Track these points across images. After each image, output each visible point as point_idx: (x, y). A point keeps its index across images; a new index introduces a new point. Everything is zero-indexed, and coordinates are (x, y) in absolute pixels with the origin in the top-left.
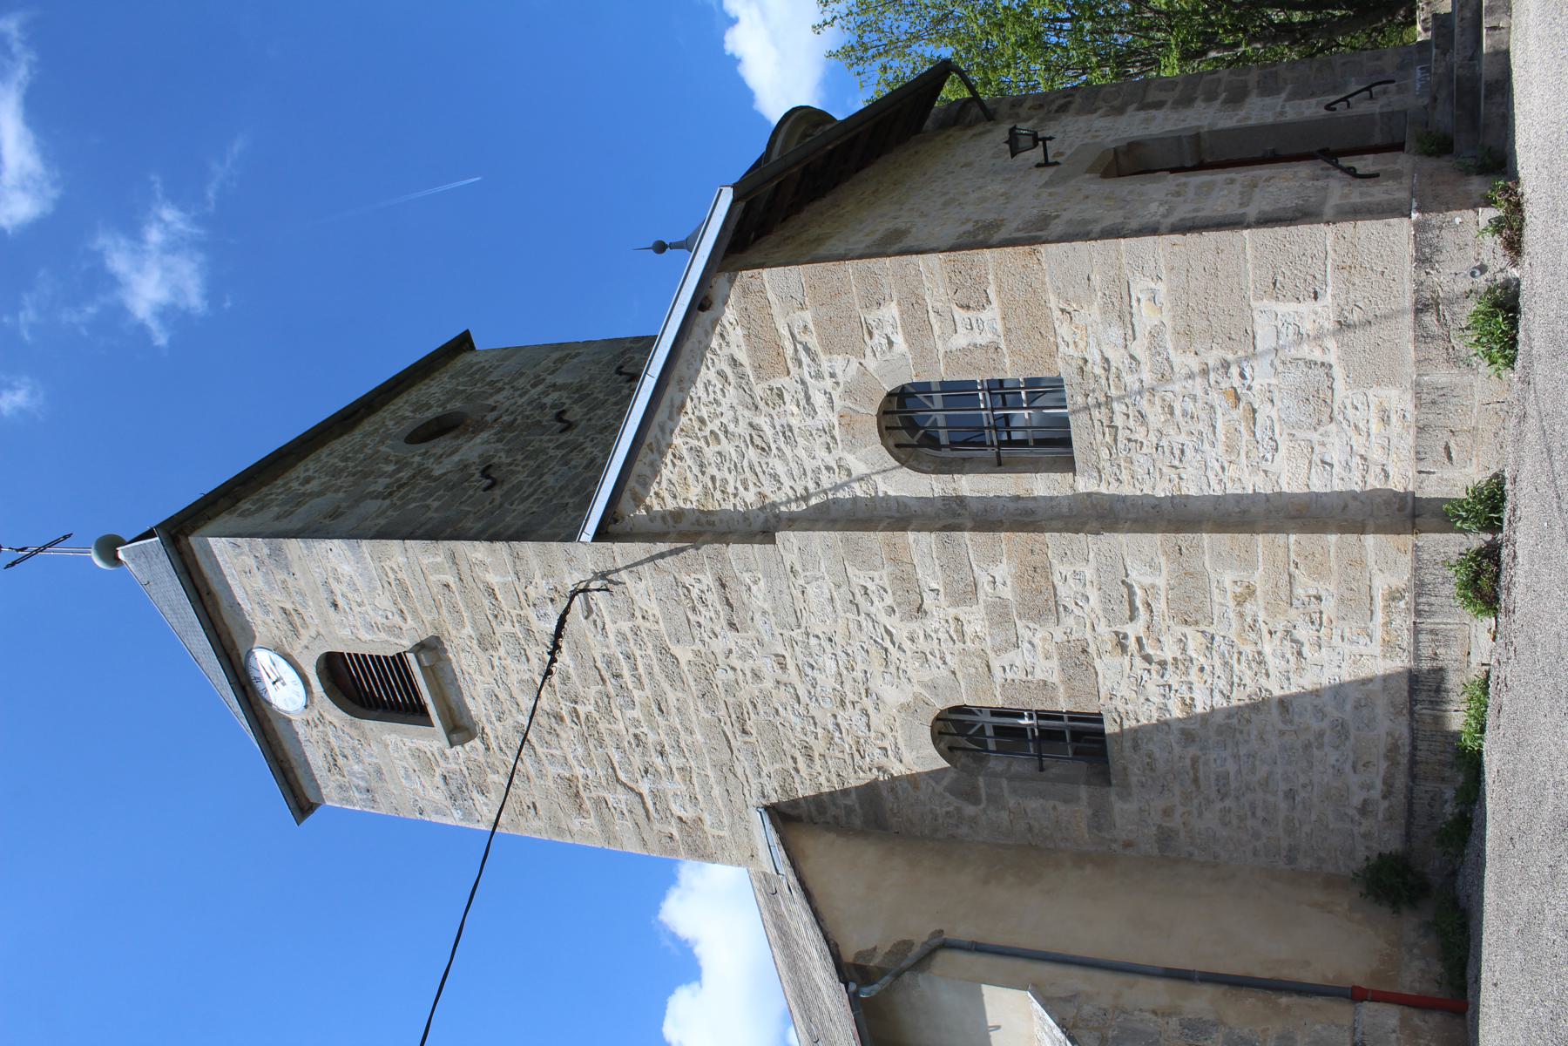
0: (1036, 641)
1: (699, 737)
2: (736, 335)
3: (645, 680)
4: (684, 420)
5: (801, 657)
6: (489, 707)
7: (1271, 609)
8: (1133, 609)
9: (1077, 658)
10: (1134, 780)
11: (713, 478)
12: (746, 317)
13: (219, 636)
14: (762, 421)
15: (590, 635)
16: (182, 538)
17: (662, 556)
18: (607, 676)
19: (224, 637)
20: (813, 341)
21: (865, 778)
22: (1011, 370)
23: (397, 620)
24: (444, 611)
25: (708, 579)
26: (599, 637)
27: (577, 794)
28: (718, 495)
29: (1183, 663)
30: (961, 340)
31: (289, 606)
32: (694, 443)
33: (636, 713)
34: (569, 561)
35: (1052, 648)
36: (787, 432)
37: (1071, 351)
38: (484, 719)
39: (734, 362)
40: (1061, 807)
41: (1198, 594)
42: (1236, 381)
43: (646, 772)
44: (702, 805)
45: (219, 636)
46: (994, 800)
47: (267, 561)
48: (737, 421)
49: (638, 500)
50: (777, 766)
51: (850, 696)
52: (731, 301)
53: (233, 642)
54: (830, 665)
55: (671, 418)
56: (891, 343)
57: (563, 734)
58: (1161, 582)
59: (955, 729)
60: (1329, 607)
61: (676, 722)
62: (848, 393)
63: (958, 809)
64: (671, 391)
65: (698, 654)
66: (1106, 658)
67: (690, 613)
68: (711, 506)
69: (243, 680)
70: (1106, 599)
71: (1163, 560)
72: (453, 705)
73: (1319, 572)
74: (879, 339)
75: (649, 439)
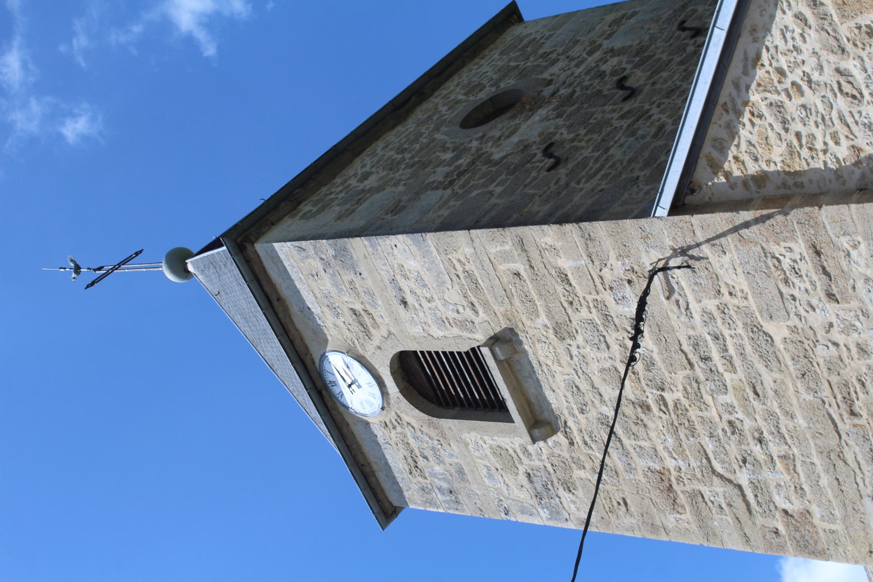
1: (801, 421)
3: (737, 362)
4: (760, 73)
6: (571, 399)
11: (798, 135)
13: (292, 342)
14: (851, 65)
15: (673, 317)
16: (248, 245)
17: (746, 225)
18: (694, 359)
19: (297, 342)
23: (469, 313)
24: (517, 302)
25: (800, 247)
26: (683, 318)
27: (670, 488)
28: (805, 153)
31: (358, 307)
32: (773, 97)
33: (729, 398)
34: (645, 238)
38: (566, 412)
43: (744, 461)
44: (809, 495)
45: (292, 342)
47: (333, 262)
48: (821, 68)
49: (716, 167)
53: (306, 347)
55: (745, 73)
57: (650, 424)
65: (794, 330)
67: (782, 286)
68: (798, 166)
69: (319, 384)
72: (533, 400)
75: (723, 98)
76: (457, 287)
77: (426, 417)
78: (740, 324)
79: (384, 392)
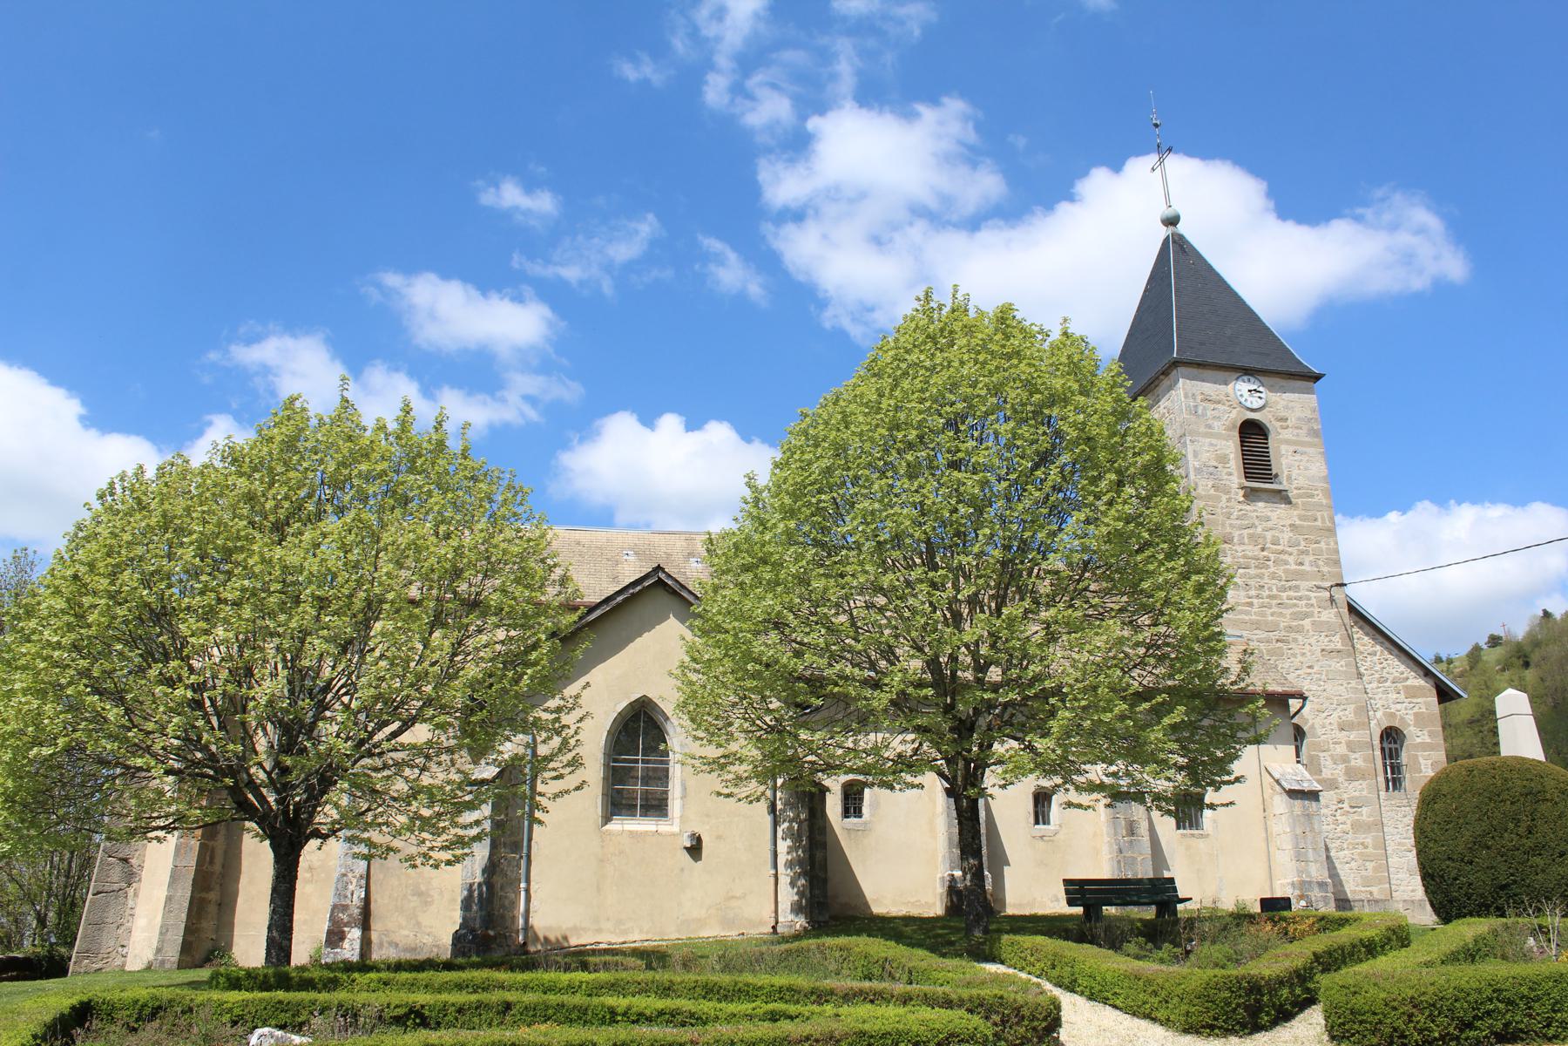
7: (1361, 854)
12: (1420, 688)
25: (1339, 646)
29: (1336, 822)
60: (1364, 873)
73: (1375, 869)
79: (1252, 410)
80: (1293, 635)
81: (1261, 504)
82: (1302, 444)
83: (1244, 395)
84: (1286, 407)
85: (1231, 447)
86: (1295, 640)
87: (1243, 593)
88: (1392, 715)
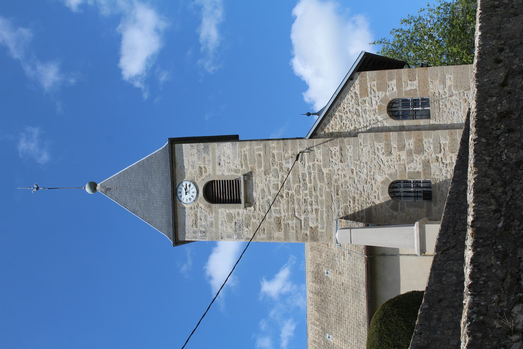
0: (418, 160)
1: (324, 197)
2: (357, 87)
3: (313, 180)
4: (340, 108)
5: (358, 169)
6: (261, 194)
8: (441, 150)
9: (426, 164)
10: (438, 199)
11: (344, 124)
12: (361, 84)
14: (359, 108)
17: (327, 141)
18: (301, 180)
20: (375, 89)
21: (369, 206)
22: (418, 96)
23: (239, 167)
24: (256, 164)
25: (338, 148)
27: (280, 223)
28: (344, 128)
30: (408, 88)
31: (202, 166)
32: (341, 114)
33: (307, 192)
34: (300, 145)
35: (421, 161)
36: (365, 111)
37: (432, 91)
39: (355, 93)
40: (419, 210)
41: (455, 145)
42: (466, 97)
44: (319, 221)
46: (402, 209)
48: (353, 108)
49: (322, 130)
50: (345, 205)
51: (369, 180)
52: (358, 79)
54: (365, 170)
55: (337, 108)
56: (393, 89)
57: (282, 201)
58: (447, 142)
59: (394, 188)
61: (318, 193)
62: (381, 101)
63: (392, 214)
64: (338, 100)
65: (330, 171)
66: (434, 163)
68: (342, 131)
69: (175, 192)
70: (435, 147)
71: (448, 136)
74: (390, 88)
75: (330, 113)
76: (240, 159)
77: (208, 203)
78: (317, 169)
80: (333, 182)
81: (255, 194)
82: (214, 159)
83: (189, 196)
84: (193, 167)
85: (223, 210)
86: (336, 181)
87: (310, 216)
88: (380, 107)
